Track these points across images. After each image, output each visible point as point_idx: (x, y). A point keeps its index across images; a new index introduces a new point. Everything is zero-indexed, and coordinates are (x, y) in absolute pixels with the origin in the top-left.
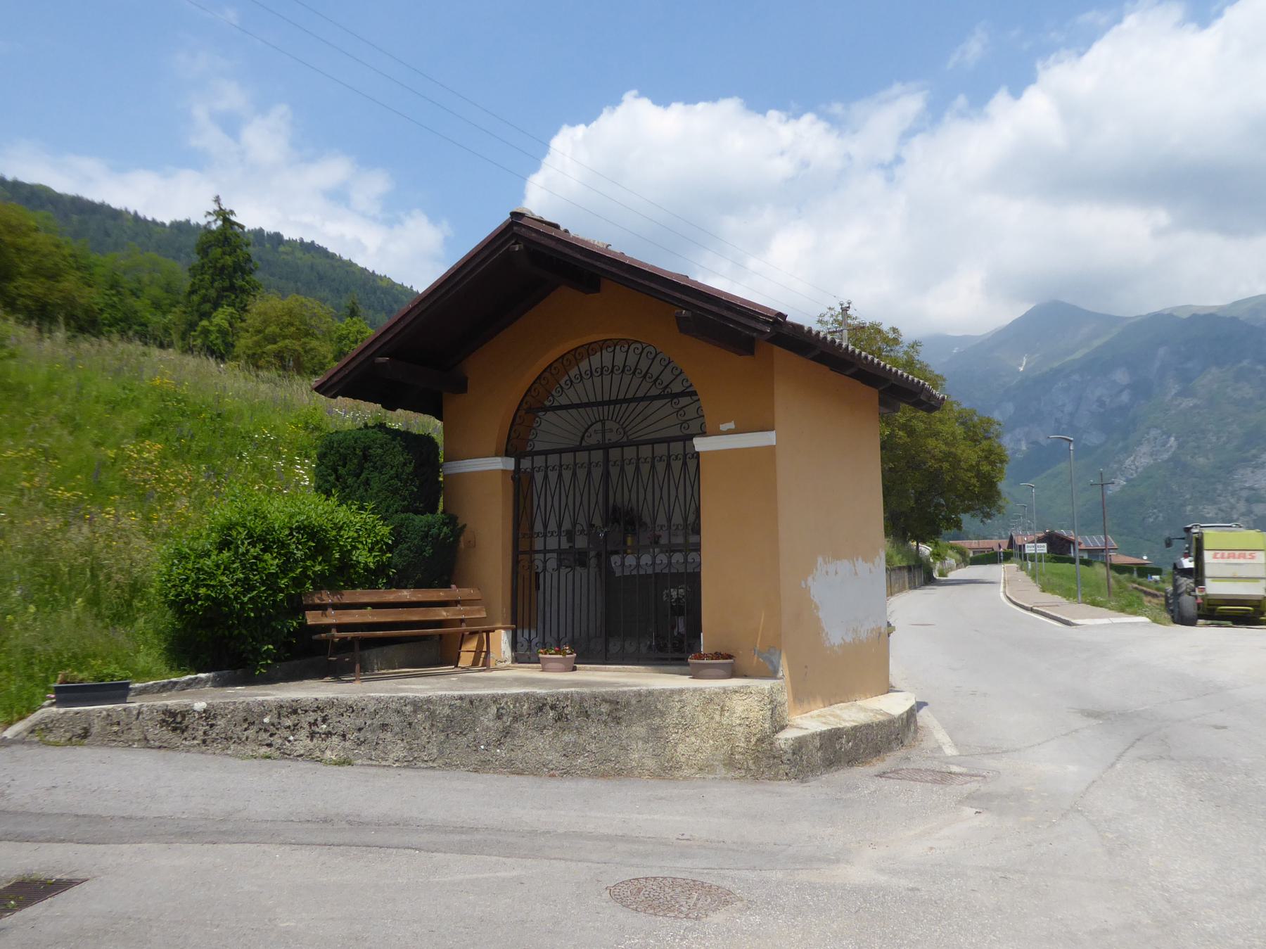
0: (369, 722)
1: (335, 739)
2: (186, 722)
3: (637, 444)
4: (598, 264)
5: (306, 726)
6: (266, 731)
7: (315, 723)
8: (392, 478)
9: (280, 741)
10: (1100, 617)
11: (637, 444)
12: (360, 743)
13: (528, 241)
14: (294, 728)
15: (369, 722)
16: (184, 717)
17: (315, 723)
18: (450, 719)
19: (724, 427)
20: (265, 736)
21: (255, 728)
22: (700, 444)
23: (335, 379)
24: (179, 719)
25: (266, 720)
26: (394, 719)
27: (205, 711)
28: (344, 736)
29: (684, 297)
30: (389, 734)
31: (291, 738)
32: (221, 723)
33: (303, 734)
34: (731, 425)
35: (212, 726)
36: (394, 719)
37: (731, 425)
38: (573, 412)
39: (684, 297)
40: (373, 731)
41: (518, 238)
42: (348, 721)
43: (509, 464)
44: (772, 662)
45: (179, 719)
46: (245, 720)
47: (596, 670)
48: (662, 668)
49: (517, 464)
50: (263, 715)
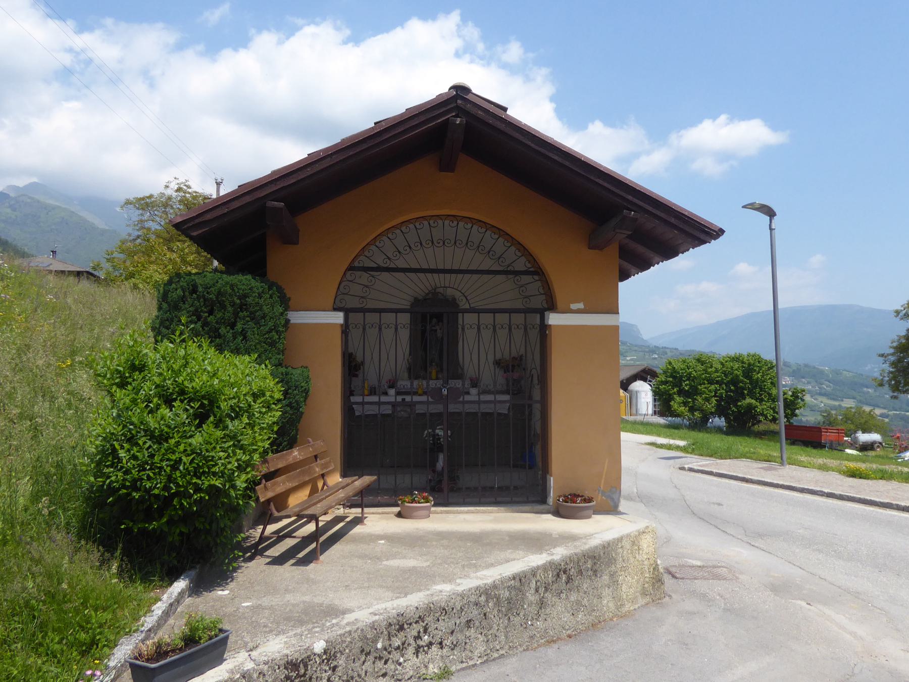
0: (458, 622)
1: (434, 648)
2: (309, 673)
3: (479, 311)
4: (551, 155)
5: (412, 641)
6: (380, 658)
7: (418, 637)
8: (270, 331)
9: (393, 667)
10: (659, 435)
11: (479, 311)
12: (454, 647)
13: (467, 113)
14: (401, 649)
15: (458, 622)
16: (306, 666)
17: (418, 637)
18: (509, 601)
19: (574, 306)
20: (380, 664)
21: (371, 658)
22: (554, 319)
23: (208, 217)
24: (302, 671)
25: (379, 646)
26: (474, 613)
27: (325, 652)
28: (441, 643)
29: (635, 200)
30: (472, 630)
31: (402, 660)
32: (341, 661)
33: (411, 650)
34: (581, 306)
35: (334, 669)
36: (474, 613)
37: (581, 306)
38: (421, 275)
39: (635, 200)
40: (461, 631)
41: (460, 111)
42: (444, 626)
43: (338, 318)
44: (612, 499)
45: (302, 671)
46: (362, 651)
47: (478, 512)
48: (515, 508)
49: (346, 318)
50: (375, 641)
